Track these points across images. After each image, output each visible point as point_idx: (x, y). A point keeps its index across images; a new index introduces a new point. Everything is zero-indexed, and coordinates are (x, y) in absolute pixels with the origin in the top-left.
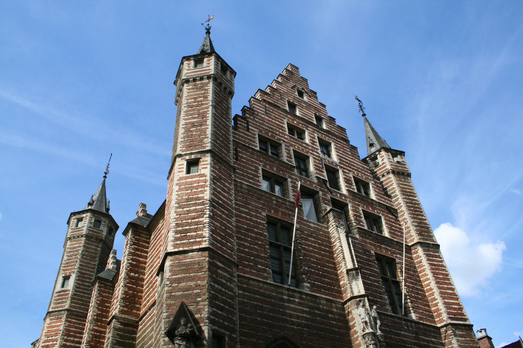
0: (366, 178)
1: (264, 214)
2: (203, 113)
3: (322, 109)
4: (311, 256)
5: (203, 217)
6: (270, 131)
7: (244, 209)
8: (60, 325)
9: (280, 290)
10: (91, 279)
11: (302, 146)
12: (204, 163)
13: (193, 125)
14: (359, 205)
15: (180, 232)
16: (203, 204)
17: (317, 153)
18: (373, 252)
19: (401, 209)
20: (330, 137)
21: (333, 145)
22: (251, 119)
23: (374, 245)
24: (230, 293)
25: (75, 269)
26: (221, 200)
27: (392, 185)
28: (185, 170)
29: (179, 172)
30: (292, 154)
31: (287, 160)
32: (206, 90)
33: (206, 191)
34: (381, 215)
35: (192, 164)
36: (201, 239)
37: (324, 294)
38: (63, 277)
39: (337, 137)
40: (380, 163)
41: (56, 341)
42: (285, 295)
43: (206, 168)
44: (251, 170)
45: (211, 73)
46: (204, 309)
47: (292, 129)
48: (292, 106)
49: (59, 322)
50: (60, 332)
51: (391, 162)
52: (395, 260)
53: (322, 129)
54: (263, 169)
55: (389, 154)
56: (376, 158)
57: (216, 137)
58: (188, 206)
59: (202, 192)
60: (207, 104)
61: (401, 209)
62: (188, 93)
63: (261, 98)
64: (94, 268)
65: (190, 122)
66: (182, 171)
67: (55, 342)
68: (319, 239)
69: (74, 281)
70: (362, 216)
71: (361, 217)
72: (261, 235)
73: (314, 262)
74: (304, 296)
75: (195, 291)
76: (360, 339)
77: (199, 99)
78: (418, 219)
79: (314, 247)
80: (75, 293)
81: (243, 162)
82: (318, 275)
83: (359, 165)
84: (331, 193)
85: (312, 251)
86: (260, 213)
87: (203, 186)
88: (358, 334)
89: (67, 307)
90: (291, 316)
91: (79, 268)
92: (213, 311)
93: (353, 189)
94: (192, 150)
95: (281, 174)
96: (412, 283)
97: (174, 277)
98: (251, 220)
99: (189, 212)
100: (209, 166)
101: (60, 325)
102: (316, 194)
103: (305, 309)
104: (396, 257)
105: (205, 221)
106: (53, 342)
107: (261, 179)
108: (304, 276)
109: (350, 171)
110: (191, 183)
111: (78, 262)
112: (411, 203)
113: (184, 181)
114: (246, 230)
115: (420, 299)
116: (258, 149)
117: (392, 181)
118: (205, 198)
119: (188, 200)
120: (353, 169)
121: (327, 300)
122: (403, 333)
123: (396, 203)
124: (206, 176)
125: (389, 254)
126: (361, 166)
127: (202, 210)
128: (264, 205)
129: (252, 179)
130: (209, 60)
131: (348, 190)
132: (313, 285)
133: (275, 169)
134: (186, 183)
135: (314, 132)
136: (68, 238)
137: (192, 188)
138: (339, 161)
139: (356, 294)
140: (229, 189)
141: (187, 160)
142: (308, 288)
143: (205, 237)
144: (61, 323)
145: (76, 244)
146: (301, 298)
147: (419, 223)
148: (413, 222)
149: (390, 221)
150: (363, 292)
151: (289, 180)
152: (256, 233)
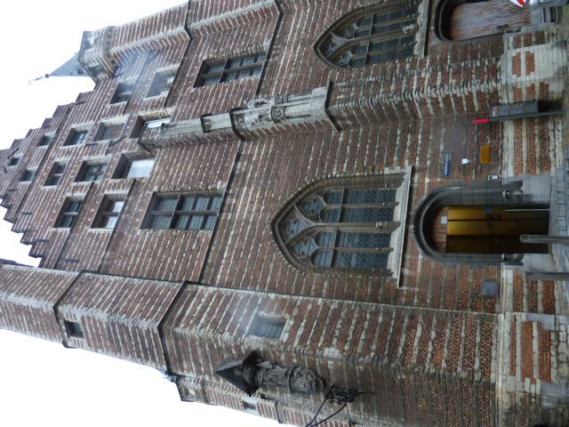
0: (113, 87)
1: (139, 232)
2: (16, 309)
4: (189, 174)
6: (51, 211)
7: (132, 259)
11: (71, 169)
13: (30, 322)
15: (146, 356)
17: (80, 149)
18: (193, 90)
21: (73, 126)
22: (35, 236)
23: (186, 87)
24: (213, 300)
26: (112, 297)
28: (80, 339)
37: (230, 163)
39: (65, 118)
40: (98, 64)
42: (227, 216)
44: (90, 244)
47: (52, 180)
48: (26, 175)
52: (204, 62)
57: (42, 296)
58: (117, 340)
68: (172, 160)
70: (153, 98)
71: (154, 101)
72: (160, 239)
73: (196, 172)
74: (231, 191)
75: (208, 349)
78: (160, 24)
79: (180, 169)
81: (81, 253)
82: (209, 169)
84: (125, 137)
85: (184, 173)
86: (138, 237)
87: (95, 322)
90: (250, 212)
92: (229, 330)
95: (98, 203)
96: (231, 41)
98: (144, 251)
99: (123, 342)
103: (244, 191)
104: (201, 58)
108: (210, 188)
114: (154, 258)
115: (249, 33)
119: (111, 341)
122: (282, 62)
125: (197, 68)
129: (100, 243)
131: (124, 113)
132: (220, 177)
133: (93, 210)
134: (94, 339)
137: (99, 336)
138: (92, 122)
139: (228, 124)
140: (103, 283)
141: (68, 336)
142: (222, 183)
150: (227, 116)
151: (106, 192)
152: (159, 246)
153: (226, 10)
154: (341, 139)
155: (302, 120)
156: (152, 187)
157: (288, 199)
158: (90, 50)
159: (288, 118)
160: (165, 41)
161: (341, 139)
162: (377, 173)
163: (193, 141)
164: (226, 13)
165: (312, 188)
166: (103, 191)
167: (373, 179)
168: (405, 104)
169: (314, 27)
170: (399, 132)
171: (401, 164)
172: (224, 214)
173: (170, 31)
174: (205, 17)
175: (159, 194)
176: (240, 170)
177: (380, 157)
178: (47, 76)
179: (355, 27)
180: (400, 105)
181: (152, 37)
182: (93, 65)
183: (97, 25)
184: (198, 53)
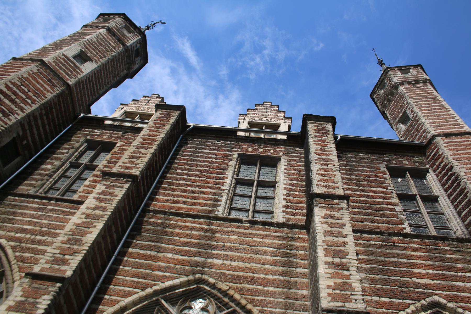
8: (48, 91)
10: (100, 89)
25: (100, 61)
38: (81, 50)
41: (32, 103)
49: (49, 86)
50: (44, 98)
64: (108, 84)
67: (29, 101)
69: (92, 71)
80: (84, 81)
89: (70, 83)
91: (103, 65)
101: (48, 91)
106: (27, 98)
111: (106, 59)
136: (108, 27)
144: (52, 91)
145: (112, 42)
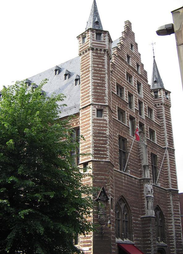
3: (137, 55)
5: (106, 145)
9: (122, 174)
12: (105, 113)
14: (148, 125)
16: (106, 137)
19: (163, 127)
20: (141, 80)
21: (142, 84)
27: (162, 112)
28: (96, 114)
29: (93, 115)
30: (128, 95)
31: (126, 99)
32: (104, 60)
33: (107, 130)
34: (155, 130)
35: (100, 112)
36: (106, 156)
39: (143, 78)
40: (159, 97)
43: (106, 116)
45: (106, 48)
46: (108, 189)
48: (128, 57)
51: (164, 98)
53: (139, 74)
54: (118, 107)
55: (164, 92)
56: (157, 92)
59: (106, 130)
60: (104, 71)
61: (163, 127)
62: (94, 58)
63: (117, 54)
65: (96, 82)
66: (95, 115)
75: (105, 181)
76: (144, 197)
77: (100, 66)
83: (150, 98)
88: (144, 195)
93: (147, 115)
94: (98, 102)
97: (95, 172)
99: (100, 140)
100: (107, 115)
102: (134, 119)
105: (107, 147)
107: (117, 113)
109: (147, 103)
110: (100, 123)
112: (168, 124)
113: (96, 121)
116: (116, 93)
117: (162, 109)
118: (107, 134)
120: (148, 101)
121: (135, 178)
123: (162, 122)
124: (106, 121)
126: (151, 99)
127: (106, 141)
128: (118, 129)
130: (104, 37)
132: (131, 171)
134: (97, 123)
135: (136, 77)
137: (100, 126)
138: (143, 97)
139: (146, 177)
143: (107, 155)
146: (128, 178)
147: (170, 137)
148: (168, 136)
149: (158, 134)
151: (126, 112)
153: (171, 167)
154: (139, 219)
155: (146, 206)
156: (128, 138)
157: (127, 201)
158: (165, 94)
159: (148, 202)
160: (164, 136)
161: (139, 219)
162: (133, 232)
163: (139, 157)
164: (170, 167)
165: (129, 209)
166: (126, 111)
167: (131, 231)
168: (150, 242)
169: (162, 204)
170: (140, 239)
171: (136, 240)
172: (123, 175)
173: (167, 139)
174: (170, 157)
175: (126, 141)
176: (132, 180)
177: (136, 233)
178: (154, 57)
179: (160, 219)
180: (149, 240)
181: (166, 130)
182: (159, 94)
183: (172, 97)
184: (159, 152)
